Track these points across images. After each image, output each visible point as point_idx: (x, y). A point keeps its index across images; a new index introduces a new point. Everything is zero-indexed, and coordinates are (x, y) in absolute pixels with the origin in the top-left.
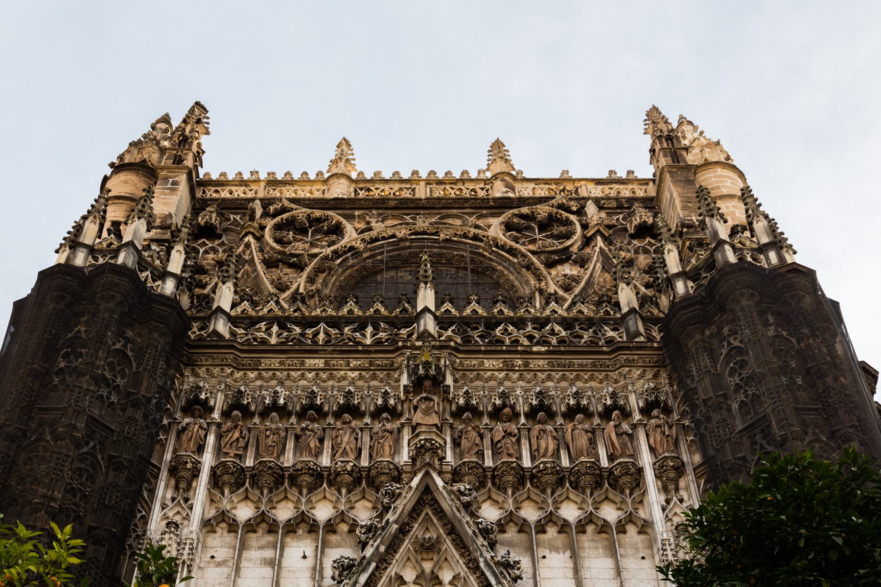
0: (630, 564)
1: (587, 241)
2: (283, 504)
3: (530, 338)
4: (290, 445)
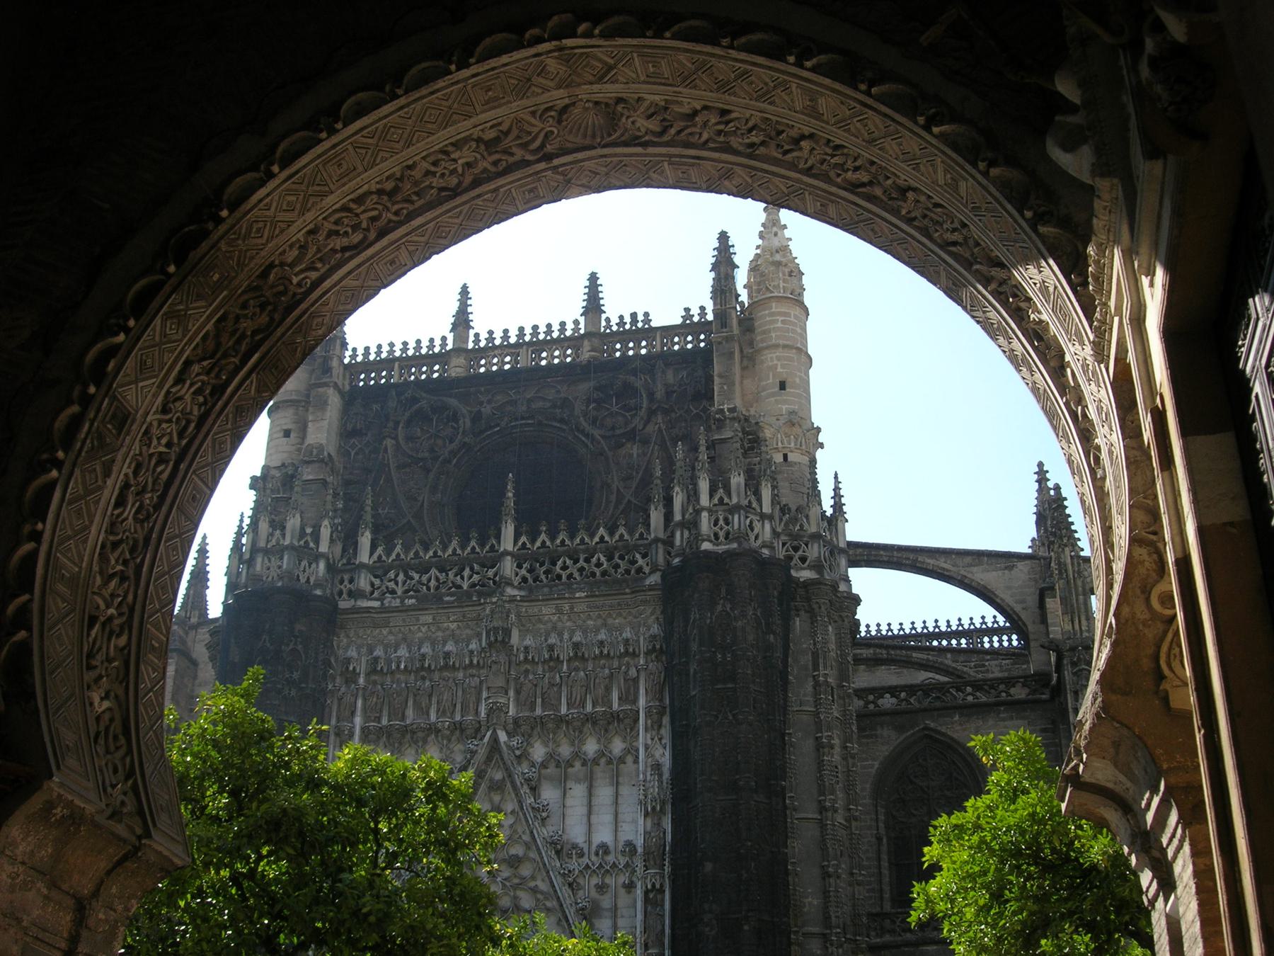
0: (625, 790)
1: (652, 413)
2: (409, 750)
3: (581, 570)
4: (410, 703)
